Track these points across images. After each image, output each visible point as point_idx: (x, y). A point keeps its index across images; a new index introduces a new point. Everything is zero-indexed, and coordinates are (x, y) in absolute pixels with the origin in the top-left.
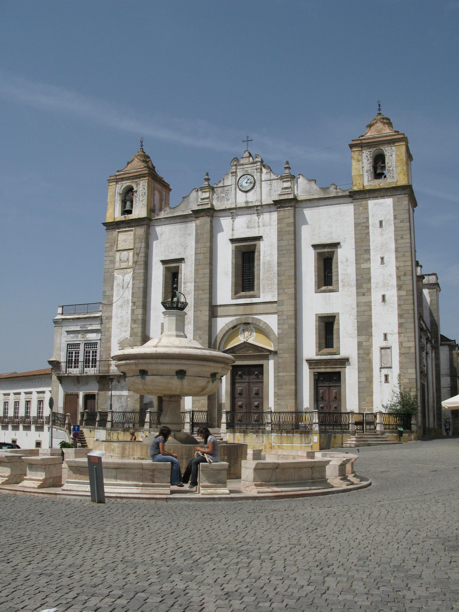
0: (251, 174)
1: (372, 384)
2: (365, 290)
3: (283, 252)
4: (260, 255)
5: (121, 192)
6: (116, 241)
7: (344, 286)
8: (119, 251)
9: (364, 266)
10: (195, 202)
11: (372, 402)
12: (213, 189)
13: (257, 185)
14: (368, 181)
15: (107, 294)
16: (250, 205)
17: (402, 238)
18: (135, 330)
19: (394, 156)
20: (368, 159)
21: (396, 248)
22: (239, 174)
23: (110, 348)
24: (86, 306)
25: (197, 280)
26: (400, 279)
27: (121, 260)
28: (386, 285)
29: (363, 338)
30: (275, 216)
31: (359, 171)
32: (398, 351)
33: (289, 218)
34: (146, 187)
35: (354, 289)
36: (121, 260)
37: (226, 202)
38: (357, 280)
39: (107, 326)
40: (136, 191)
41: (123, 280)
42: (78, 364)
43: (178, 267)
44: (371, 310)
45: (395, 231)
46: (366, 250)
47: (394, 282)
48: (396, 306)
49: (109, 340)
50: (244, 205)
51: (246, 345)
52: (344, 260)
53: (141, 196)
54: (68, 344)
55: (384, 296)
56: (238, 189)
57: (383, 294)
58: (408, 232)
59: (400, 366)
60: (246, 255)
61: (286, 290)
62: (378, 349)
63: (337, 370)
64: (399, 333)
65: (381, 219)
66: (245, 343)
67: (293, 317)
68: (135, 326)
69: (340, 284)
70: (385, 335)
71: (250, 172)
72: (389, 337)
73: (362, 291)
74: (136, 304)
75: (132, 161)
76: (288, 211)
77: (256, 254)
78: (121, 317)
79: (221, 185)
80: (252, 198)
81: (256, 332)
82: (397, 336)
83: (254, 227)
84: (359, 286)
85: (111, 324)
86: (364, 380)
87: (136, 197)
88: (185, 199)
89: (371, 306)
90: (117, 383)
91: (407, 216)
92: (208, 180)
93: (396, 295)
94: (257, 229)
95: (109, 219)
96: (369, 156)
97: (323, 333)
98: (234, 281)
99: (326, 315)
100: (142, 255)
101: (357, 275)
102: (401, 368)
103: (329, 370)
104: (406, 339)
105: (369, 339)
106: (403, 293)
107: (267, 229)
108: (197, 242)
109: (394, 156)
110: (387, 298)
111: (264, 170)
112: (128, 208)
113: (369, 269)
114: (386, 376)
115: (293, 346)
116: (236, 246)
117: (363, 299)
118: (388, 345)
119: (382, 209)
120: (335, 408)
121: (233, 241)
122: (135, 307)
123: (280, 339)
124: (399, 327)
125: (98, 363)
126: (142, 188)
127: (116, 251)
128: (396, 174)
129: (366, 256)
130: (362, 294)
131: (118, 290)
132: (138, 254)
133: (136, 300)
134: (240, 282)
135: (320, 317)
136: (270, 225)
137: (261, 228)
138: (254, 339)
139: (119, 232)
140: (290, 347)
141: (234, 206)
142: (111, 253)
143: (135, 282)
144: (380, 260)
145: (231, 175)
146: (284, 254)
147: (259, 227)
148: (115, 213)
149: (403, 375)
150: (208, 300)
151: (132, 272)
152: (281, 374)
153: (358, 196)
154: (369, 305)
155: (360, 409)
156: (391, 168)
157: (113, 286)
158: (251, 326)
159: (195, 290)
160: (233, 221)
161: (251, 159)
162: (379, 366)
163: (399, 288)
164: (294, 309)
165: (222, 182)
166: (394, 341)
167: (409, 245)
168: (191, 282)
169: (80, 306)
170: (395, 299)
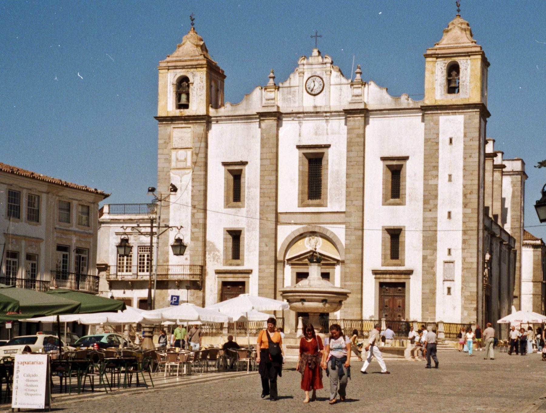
0: (321, 76)
2: (432, 206)
3: (352, 164)
4: (328, 164)
5: (175, 83)
7: (411, 200)
8: (176, 149)
9: (432, 182)
10: (259, 102)
14: (441, 95)
16: (318, 110)
17: (470, 156)
18: (196, 235)
19: (469, 70)
20: (442, 72)
21: (464, 166)
24: (138, 206)
26: (466, 197)
27: (177, 159)
29: (428, 252)
32: (461, 266)
33: (359, 128)
35: (420, 204)
36: (177, 159)
38: (424, 196)
42: (130, 267)
43: (241, 171)
44: (436, 226)
45: (465, 149)
46: (434, 167)
47: (460, 199)
53: (199, 89)
55: (449, 213)
58: (477, 151)
59: (462, 279)
60: (314, 161)
61: (354, 202)
62: (442, 263)
63: (402, 281)
64: (463, 249)
65: (451, 136)
68: (196, 230)
70: (449, 250)
71: (318, 73)
73: (429, 207)
80: (320, 101)
82: (461, 251)
84: (426, 202)
86: (428, 291)
89: (437, 222)
96: (443, 68)
98: (301, 189)
99: (392, 228)
101: (424, 191)
102: (463, 282)
103: (393, 281)
105: (434, 253)
108: (262, 146)
109: (469, 70)
113: (437, 186)
114: (449, 289)
115: (360, 258)
116: (304, 154)
117: (429, 215)
118: (452, 260)
119: (453, 125)
121: (299, 147)
122: (195, 211)
123: (347, 250)
128: (470, 90)
129: (434, 173)
130: (428, 210)
132: (197, 154)
133: (196, 203)
134: (306, 190)
139: (174, 128)
140: (357, 258)
141: (301, 111)
142: (166, 151)
143: (195, 184)
146: (352, 166)
147: (327, 134)
148: (168, 105)
149: (465, 288)
150: (274, 208)
151: (191, 173)
152: (348, 283)
154: (435, 220)
155: (423, 319)
156: (465, 84)
158: (318, 235)
159: (261, 197)
160: (300, 126)
162: (442, 280)
163: (465, 205)
165: (288, 81)
166: (457, 256)
167: (477, 164)
169: (130, 206)
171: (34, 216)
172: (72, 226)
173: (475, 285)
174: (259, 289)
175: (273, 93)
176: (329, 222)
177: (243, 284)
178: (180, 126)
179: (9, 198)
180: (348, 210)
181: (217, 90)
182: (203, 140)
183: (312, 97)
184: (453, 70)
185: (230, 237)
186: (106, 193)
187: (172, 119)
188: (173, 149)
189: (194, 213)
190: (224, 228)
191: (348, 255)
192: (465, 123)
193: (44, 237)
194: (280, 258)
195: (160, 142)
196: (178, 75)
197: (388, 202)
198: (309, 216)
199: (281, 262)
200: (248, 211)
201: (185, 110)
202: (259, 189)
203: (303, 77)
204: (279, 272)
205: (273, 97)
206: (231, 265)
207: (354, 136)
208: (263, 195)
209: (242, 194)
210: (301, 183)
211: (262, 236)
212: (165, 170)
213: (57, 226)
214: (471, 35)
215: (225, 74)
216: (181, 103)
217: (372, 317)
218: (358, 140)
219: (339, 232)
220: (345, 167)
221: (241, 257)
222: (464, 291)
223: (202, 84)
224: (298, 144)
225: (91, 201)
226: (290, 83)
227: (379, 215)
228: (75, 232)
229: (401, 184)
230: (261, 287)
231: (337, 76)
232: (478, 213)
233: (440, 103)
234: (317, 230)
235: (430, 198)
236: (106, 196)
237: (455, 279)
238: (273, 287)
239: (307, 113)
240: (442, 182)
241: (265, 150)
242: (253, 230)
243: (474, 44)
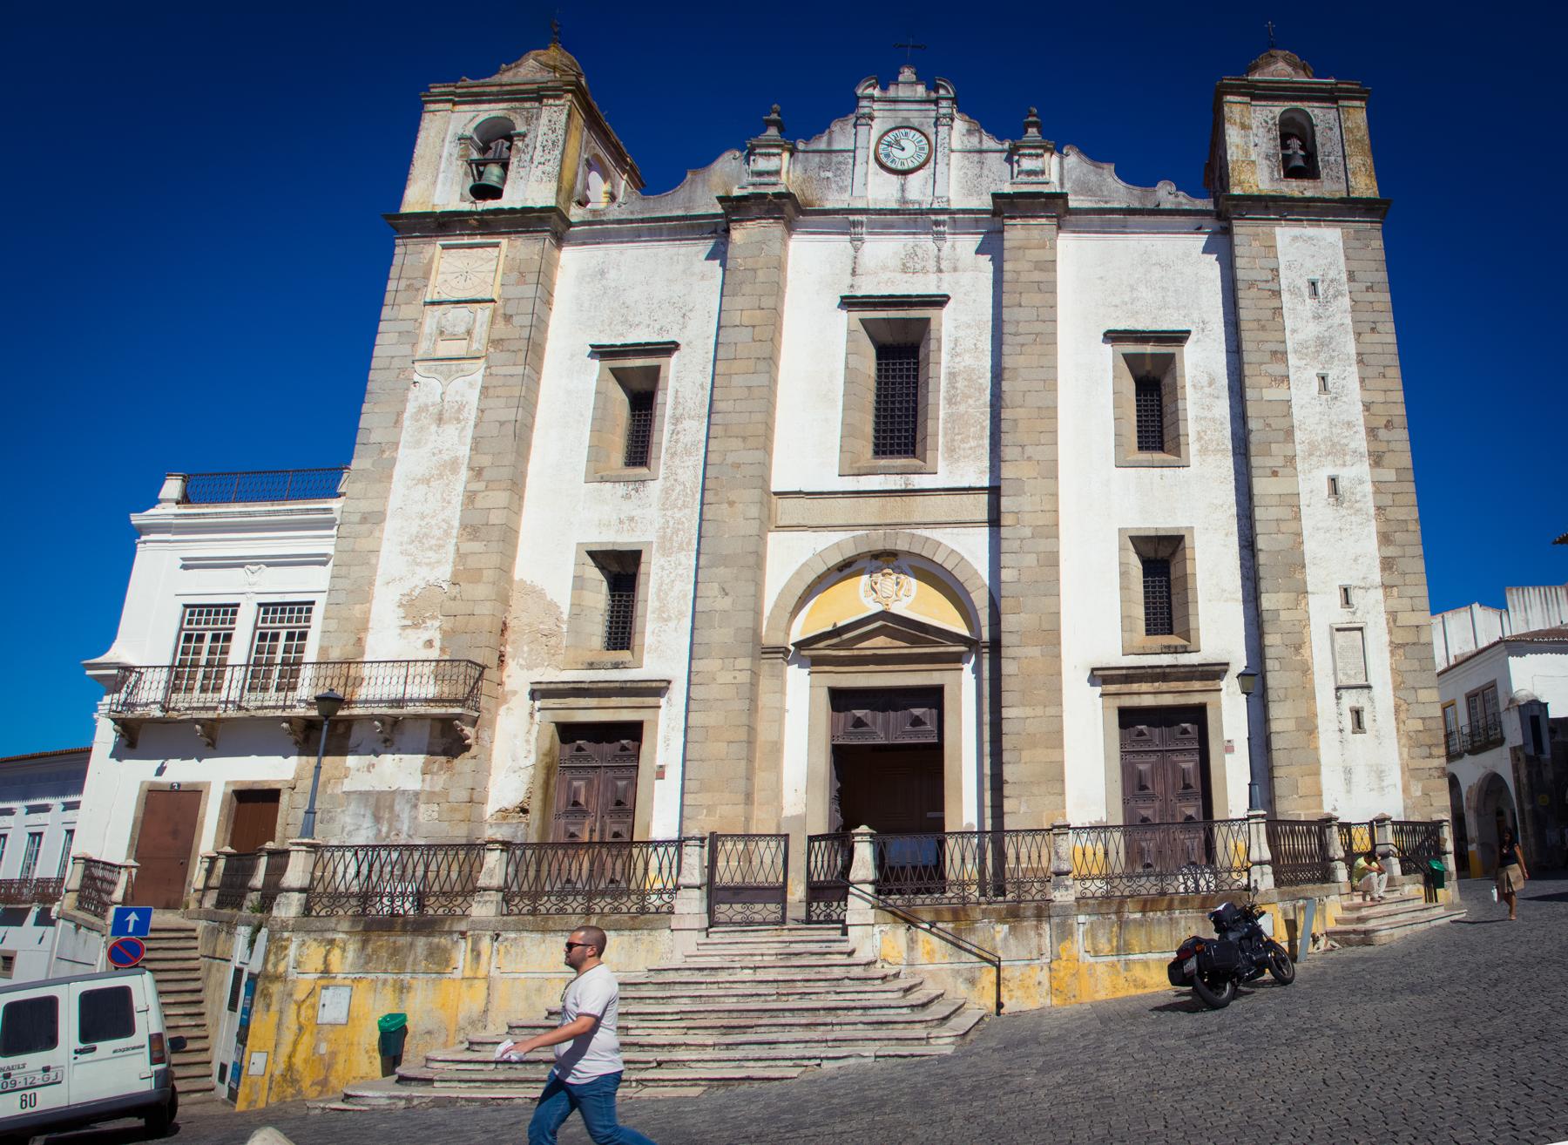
8: (440, 303)
14: (1272, 179)
23: (367, 621)
31: (1246, 152)
32: (1386, 638)
49: (362, 593)
62: (1327, 636)
64: (1386, 587)
66: (884, 615)
72: (1355, 597)
94: (933, 277)
102: (1396, 688)
103: (1167, 700)
121: (848, 303)
127: (426, 304)
138: (914, 600)
139: (445, 247)
142: (407, 311)
143: (490, 403)
156: (1332, 159)
158: (903, 562)
162: (1333, 686)
166: (1372, 608)
176: (944, 519)
178: (466, 240)
185: (594, 574)
187: (442, 224)
188: (433, 303)
189: (475, 493)
195: (391, 285)
198: (875, 502)
218: (1037, 276)
234: (902, 545)
237: (1372, 682)
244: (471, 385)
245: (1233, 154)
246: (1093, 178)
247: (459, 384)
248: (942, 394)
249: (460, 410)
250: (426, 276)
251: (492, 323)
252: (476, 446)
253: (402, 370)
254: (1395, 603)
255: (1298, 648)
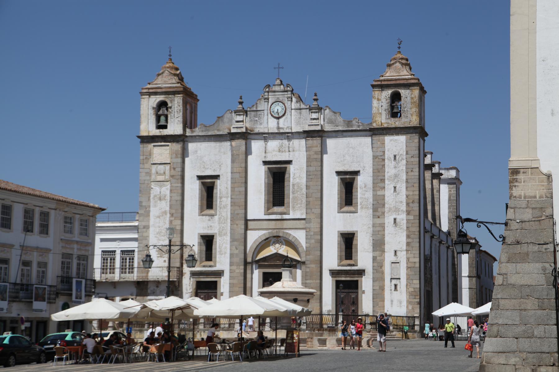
1: (384, 292)
2: (380, 214)
3: (311, 177)
5: (155, 106)
6: (150, 154)
7: (362, 208)
9: (379, 193)
11: (384, 307)
12: (246, 112)
13: (288, 111)
15: (144, 204)
16: (282, 131)
17: (412, 171)
19: (409, 98)
21: (406, 179)
22: (271, 101)
24: (121, 214)
25: (233, 197)
26: (409, 206)
28: (397, 210)
29: (377, 253)
30: (303, 142)
31: (378, 110)
32: (405, 265)
33: (317, 146)
34: (181, 103)
35: (371, 211)
37: (258, 126)
39: (145, 234)
40: (171, 107)
41: (160, 192)
43: (214, 182)
44: (384, 230)
45: (406, 165)
46: (381, 180)
47: (404, 207)
48: (405, 228)
50: (276, 131)
51: (277, 256)
52: (363, 186)
54: (102, 251)
55: (395, 219)
56: (270, 115)
57: (395, 217)
60: (278, 175)
61: (313, 210)
63: (356, 279)
64: (407, 250)
65: (395, 154)
67: (319, 233)
69: (359, 207)
71: (281, 99)
72: (398, 253)
73: (378, 214)
74: (174, 215)
75: (163, 73)
76: (316, 142)
77: (287, 176)
78: (159, 227)
79: (255, 109)
81: (286, 245)
83: (285, 151)
84: (375, 210)
85: (149, 233)
86: (377, 288)
87: (170, 113)
88: (220, 119)
90: (155, 288)
91: (417, 152)
92: (241, 103)
93: (405, 218)
94: (287, 153)
95: (144, 133)
97: (344, 247)
100: (179, 169)
102: (407, 279)
103: (348, 279)
104: (412, 255)
106: (411, 217)
107: (297, 154)
108: (233, 161)
110: (397, 220)
111: (294, 99)
112: (162, 122)
114: (396, 285)
115: (319, 259)
116: (269, 168)
117: (378, 221)
119: (396, 144)
120: (353, 311)
121: (265, 163)
122: (173, 219)
124: (407, 246)
125: (136, 270)
126: (176, 104)
129: (381, 185)
131: (156, 202)
133: (173, 211)
134: (271, 199)
135: (341, 234)
136: (300, 151)
137: (291, 153)
138: (283, 250)
139: (154, 146)
141: (266, 131)
142: (146, 166)
143: (173, 194)
144: (393, 189)
145: (263, 100)
147: (289, 151)
148: (148, 127)
150: (244, 216)
152: (308, 281)
153: (377, 132)
154: (383, 226)
157: (149, 197)
159: (231, 206)
160: (266, 144)
161: (282, 86)
162: (390, 278)
163: (408, 213)
164: (319, 226)
166: (402, 257)
167: (418, 177)
168: (227, 197)
170: (405, 221)
171: (44, 229)
172: (74, 237)
173: (418, 282)
174: (230, 287)
175: (242, 116)
177: (216, 282)
179: (25, 215)
180: (308, 217)
181: (191, 113)
182: (179, 156)
183: (275, 120)
184: (396, 98)
186: (103, 207)
188: (154, 164)
190: (199, 234)
191: (308, 257)
192: (406, 143)
193: (52, 248)
194: (249, 260)
196: (158, 100)
197: (342, 210)
198: (273, 222)
199: (250, 263)
200: (220, 219)
201: (164, 130)
202: (229, 199)
203: (268, 102)
204: (249, 272)
205: (242, 120)
206: (204, 266)
207: (312, 153)
208: (233, 204)
209: (214, 203)
210: (267, 193)
211: (233, 240)
212: (146, 182)
213: (63, 237)
214: (410, 69)
215: (198, 98)
216: (160, 124)
217: (329, 311)
218: (315, 156)
219: (300, 236)
220: (305, 179)
221: (213, 259)
222: (408, 287)
223: (179, 108)
224: (264, 160)
225: (91, 215)
226: (256, 108)
227: (335, 222)
228: (77, 242)
229: (354, 194)
230: (231, 285)
231: (297, 102)
232: (420, 219)
233: (385, 126)
234: (281, 235)
235: (378, 206)
236: (103, 210)
238: (242, 285)
239: (272, 133)
240: (388, 193)
241: (235, 164)
242: (224, 235)
243: (412, 77)
244: (167, 189)
245: (374, 110)
246: (333, 117)
247: (164, 189)
248: (291, 191)
249: (165, 197)
250: (150, 155)
251: (170, 170)
252: (171, 207)
253: (148, 184)
254: (409, 255)
255: (381, 267)
